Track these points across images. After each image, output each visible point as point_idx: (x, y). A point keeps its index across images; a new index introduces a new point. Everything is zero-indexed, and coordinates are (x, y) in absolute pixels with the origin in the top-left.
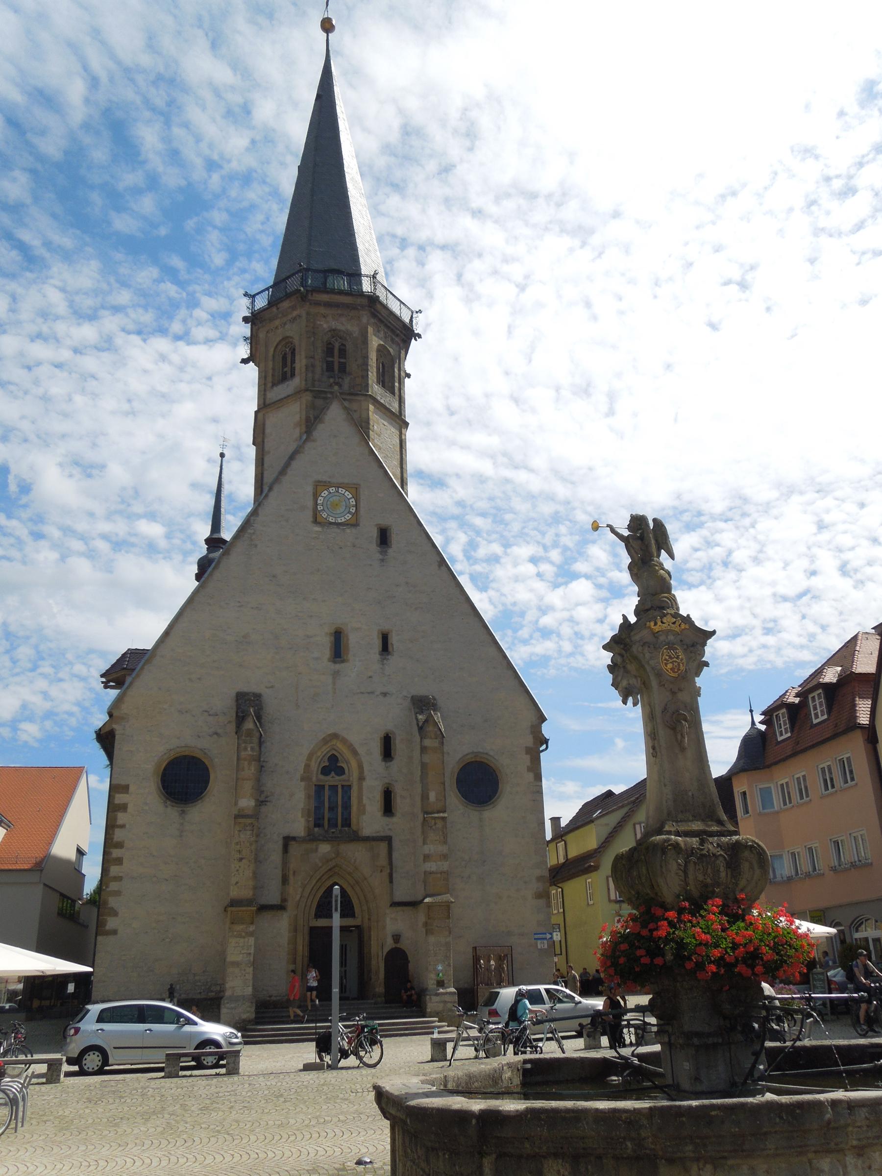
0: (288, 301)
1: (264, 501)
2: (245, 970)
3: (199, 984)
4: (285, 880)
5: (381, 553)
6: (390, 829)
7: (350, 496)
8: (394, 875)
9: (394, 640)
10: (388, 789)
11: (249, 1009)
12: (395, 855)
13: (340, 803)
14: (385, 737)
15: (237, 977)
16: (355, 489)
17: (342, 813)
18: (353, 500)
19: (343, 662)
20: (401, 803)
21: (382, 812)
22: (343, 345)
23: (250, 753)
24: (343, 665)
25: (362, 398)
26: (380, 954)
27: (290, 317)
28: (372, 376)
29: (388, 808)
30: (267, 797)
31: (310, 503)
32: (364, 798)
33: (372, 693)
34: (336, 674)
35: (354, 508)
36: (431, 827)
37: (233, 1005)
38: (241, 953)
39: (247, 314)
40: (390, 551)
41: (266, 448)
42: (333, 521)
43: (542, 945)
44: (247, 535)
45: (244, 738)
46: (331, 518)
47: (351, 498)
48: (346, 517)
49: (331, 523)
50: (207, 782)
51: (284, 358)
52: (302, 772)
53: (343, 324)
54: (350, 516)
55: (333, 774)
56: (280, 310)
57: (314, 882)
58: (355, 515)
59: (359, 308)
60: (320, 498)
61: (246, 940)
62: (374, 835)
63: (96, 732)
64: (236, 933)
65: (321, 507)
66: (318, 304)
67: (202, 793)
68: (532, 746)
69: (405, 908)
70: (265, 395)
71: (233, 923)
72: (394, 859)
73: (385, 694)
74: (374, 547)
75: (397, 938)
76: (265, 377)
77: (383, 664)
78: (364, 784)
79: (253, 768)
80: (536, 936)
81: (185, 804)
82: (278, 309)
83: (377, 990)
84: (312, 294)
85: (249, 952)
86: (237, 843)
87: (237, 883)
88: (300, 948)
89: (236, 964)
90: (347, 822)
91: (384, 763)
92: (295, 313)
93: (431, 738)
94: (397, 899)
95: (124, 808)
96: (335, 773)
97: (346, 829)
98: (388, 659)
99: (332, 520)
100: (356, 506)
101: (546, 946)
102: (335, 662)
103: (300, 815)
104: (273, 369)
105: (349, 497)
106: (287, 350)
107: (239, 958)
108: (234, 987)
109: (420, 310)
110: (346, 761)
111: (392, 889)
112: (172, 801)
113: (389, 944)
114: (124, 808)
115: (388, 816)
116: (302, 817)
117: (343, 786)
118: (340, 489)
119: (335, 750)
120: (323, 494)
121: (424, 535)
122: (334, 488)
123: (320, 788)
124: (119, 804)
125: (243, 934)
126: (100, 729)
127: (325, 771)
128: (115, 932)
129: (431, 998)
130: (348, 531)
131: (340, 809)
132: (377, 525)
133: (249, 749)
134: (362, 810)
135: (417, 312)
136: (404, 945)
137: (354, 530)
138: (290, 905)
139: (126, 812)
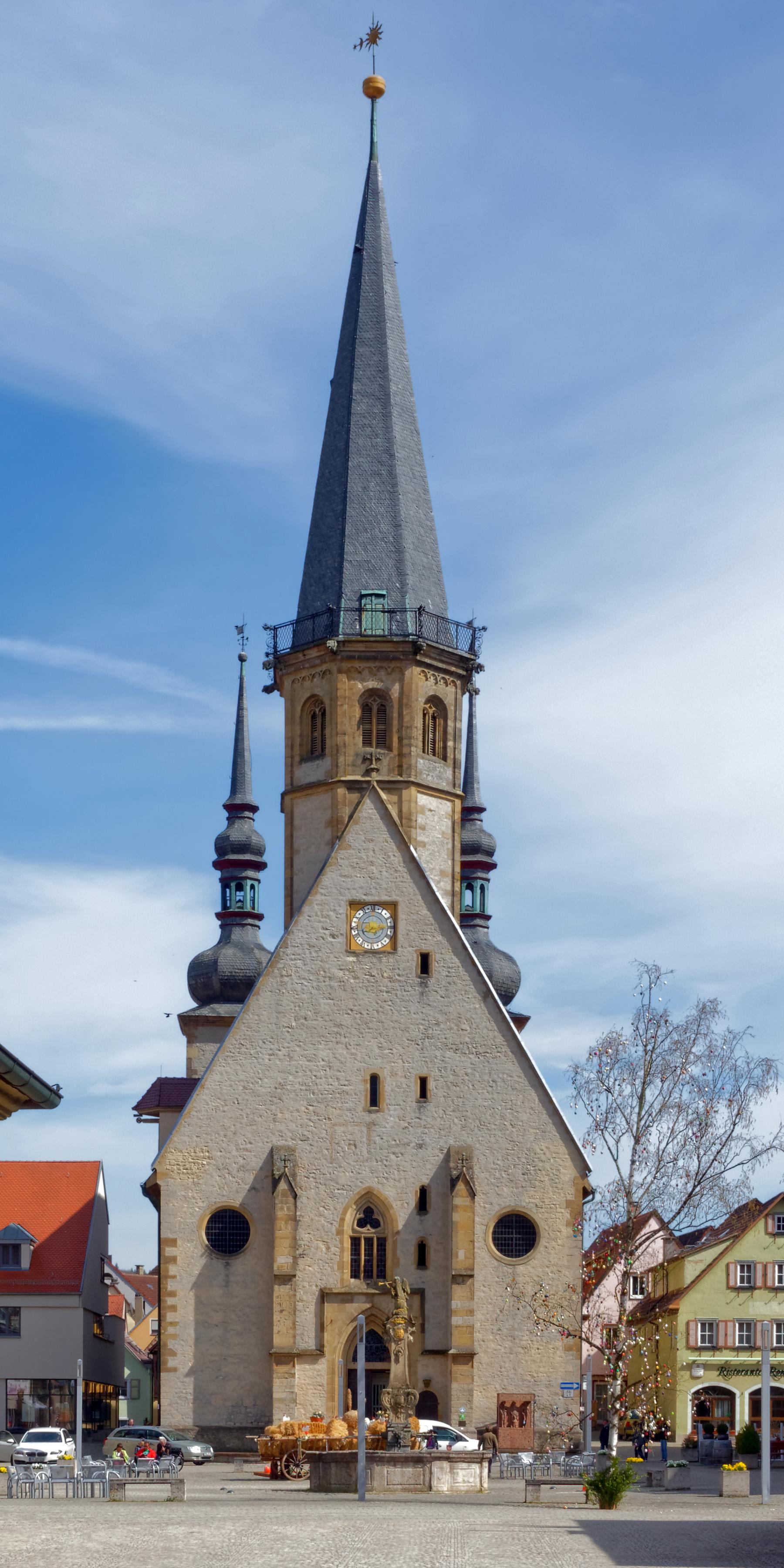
0: (316, 649)
3: (250, 1415)
4: (321, 1328)
6: (423, 1282)
8: (426, 1325)
9: (431, 1085)
10: (422, 1242)
12: (428, 1307)
16: (392, 906)
19: (377, 1111)
20: (432, 1256)
22: (382, 705)
24: (378, 1115)
25: (404, 785)
27: (318, 670)
28: (416, 749)
29: (422, 1261)
31: (343, 928)
32: (398, 1252)
34: (371, 1125)
40: (432, 982)
47: (388, 918)
48: (383, 941)
49: (367, 952)
50: (248, 1235)
51: (314, 717)
52: (337, 1226)
55: (368, 1227)
56: (307, 657)
59: (402, 657)
61: (289, 1380)
63: (141, 1186)
66: (350, 658)
67: (244, 1245)
69: (437, 1357)
70: (292, 771)
72: (426, 1312)
73: (420, 1146)
75: (427, 1382)
76: (292, 747)
77: (420, 1113)
79: (289, 1227)
80: (563, 1386)
81: (229, 1256)
82: (304, 655)
84: (344, 645)
88: (336, 1387)
89: (281, 1400)
90: (382, 1275)
91: (418, 1217)
92: (324, 667)
93: (463, 1197)
94: (430, 1346)
95: (173, 1260)
96: (371, 1226)
98: (425, 1107)
99: (367, 946)
101: (572, 1395)
102: (370, 1112)
103: (336, 1267)
104: (301, 736)
105: (386, 917)
106: (317, 710)
107: (283, 1395)
110: (381, 1213)
111: (424, 1338)
112: (217, 1254)
114: (173, 1260)
116: (338, 1269)
117: (378, 1239)
119: (371, 1203)
120: (357, 915)
121: (469, 961)
122: (369, 907)
123: (355, 1241)
126: (145, 1184)
127: (361, 1223)
128: (175, 1370)
130: (384, 959)
132: (416, 951)
134: (396, 1264)
136: (434, 1388)
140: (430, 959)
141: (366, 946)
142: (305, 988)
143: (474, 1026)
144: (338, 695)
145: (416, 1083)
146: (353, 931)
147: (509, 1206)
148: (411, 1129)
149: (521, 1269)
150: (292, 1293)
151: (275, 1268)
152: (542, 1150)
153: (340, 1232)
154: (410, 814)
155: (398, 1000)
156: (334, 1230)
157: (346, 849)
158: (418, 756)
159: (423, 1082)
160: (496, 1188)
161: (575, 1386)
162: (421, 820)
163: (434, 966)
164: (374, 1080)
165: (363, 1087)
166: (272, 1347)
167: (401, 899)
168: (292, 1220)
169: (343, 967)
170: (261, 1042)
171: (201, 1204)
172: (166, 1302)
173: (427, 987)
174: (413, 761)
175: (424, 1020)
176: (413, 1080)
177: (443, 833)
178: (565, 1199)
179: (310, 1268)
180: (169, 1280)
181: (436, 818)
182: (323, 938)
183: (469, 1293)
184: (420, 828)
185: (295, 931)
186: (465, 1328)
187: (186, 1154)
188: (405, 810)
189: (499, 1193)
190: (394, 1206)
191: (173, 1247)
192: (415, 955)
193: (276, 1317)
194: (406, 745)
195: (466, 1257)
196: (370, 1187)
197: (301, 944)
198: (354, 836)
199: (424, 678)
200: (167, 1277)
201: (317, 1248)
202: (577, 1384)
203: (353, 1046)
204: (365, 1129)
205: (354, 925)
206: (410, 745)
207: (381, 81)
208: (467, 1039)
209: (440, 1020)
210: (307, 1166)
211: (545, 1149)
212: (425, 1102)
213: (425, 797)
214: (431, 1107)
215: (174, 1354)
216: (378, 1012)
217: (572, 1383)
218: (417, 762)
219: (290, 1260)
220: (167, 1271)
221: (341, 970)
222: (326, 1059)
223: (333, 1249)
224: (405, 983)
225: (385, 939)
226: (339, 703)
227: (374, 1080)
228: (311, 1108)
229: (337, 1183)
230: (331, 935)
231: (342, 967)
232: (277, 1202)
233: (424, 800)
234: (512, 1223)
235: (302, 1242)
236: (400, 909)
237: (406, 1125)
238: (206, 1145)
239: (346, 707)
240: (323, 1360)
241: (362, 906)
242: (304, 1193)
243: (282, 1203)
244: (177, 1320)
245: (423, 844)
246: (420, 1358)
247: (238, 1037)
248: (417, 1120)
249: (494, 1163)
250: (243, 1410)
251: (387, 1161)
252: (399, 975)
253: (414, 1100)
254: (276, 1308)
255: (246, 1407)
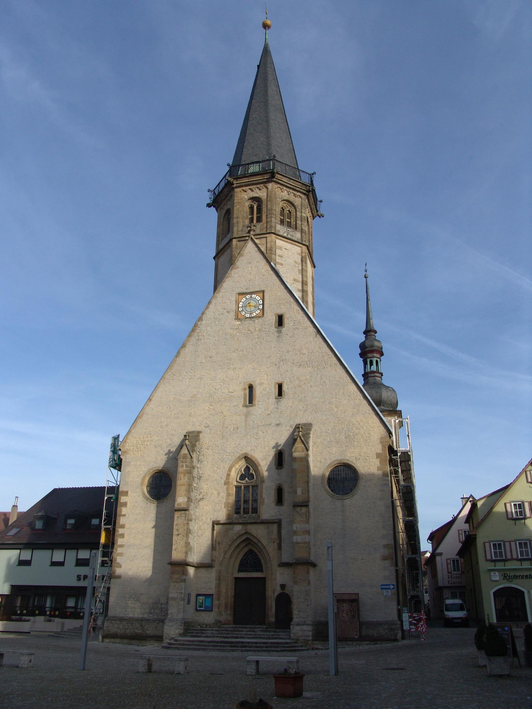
1: (206, 311)
2: (179, 603)
5: (278, 332)
7: (259, 298)
8: (283, 545)
9: (285, 388)
10: (280, 487)
11: (180, 627)
12: (283, 532)
13: (251, 498)
14: (278, 453)
15: (174, 607)
17: (252, 504)
18: (261, 301)
20: (286, 496)
21: (275, 503)
23: (185, 468)
24: (252, 408)
26: (273, 597)
29: (279, 500)
30: (203, 496)
31: (234, 307)
33: (270, 425)
34: (247, 415)
35: (262, 306)
36: (298, 512)
37: (171, 624)
38: (177, 593)
39: (209, 201)
40: (284, 330)
41: (218, 279)
42: (249, 316)
43: (387, 593)
44: (196, 334)
45: (182, 460)
46: (247, 314)
47: (260, 300)
49: (246, 318)
52: (225, 479)
53: (257, 193)
54: (259, 311)
57: (233, 549)
58: (262, 311)
60: (241, 303)
62: (270, 518)
64: (174, 580)
65: (242, 308)
68: (381, 452)
71: (172, 573)
73: (278, 425)
74: (273, 329)
75: (283, 586)
77: (278, 405)
78: (264, 484)
79: (186, 478)
80: (383, 587)
83: (270, 619)
85: (181, 592)
86: (177, 524)
87: (176, 549)
89: (174, 599)
90: (255, 510)
97: (254, 515)
98: (281, 401)
99: (248, 315)
100: (263, 304)
101: (390, 594)
102: (247, 406)
103: (223, 506)
105: (258, 299)
108: (172, 613)
109: (314, 172)
113: (278, 590)
115: (279, 505)
116: (225, 508)
117: (253, 486)
118: (253, 295)
120: (242, 301)
122: (249, 295)
124: (123, 502)
125: (178, 581)
127: (242, 477)
129: (293, 627)
130: (257, 321)
131: (250, 502)
132: (275, 314)
133: (184, 466)
135: (313, 174)
137: (260, 320)
138: (216, 564)
139: (126, 507)
140: (283, 317)
141: (247, 316)
142: (211, 341)
143: (310, 351)
144: (235, 202)
145: (275, 388)
146: (240, 309)
147: (337, 460)
148: (272, 414)
149: (347, 502)
150: (185, 522)
151: (176, 506)
152: (358, 422)
153: (227, 483)
154: (271, 247)
155: (264, 342)
156: (223, 482)
157: (236, 269)
158: (276, 223)
159: (280, 386)
160: (328, 449)
161: (392, 587)
162: (278, 252)
163: (286, 321)
164: (251, 387)
165: (243, 393)
166: (171, 559)
167: (266, 289)
168: (188, 473)
169: (233, 328)
170: (185, 373)
171: (144, 469)
172: (118, 531)
173: (281, 333)
174: (273, 224)
175: (280, 351)
176: (273, 386)
177: (295, 262)
178: (375, 452)
179: (207, 508)
180: (121, 518)
181: (290, 253)
182: (222, 314)
183: (305, 519)
184: (279, 256)
185: (207, 312)
186: (303, 544)
187: (138, 439)
188: (269, 246)
189: (330, 451)
190: (261, 464)
191: (125, 496)
192: (274, 317)
193: (175, 538)
194: (269, 217)
195: (302, 493)
196: (246, 453)
197: (210, 319)
198: (241, 262)
199: (281, 191)
200: (121, 515)
201: (212, 494)
202: (393, 585)
203: (237, 370)
204: (243, 418)
205: (240, 306)
206: (271, 217)
207: (269, 22)
208: (306, 359)
209: (290, 350)
210: (208, 443)
211: (359, 421)
212: (281, 398)
213: (282, 242)
214: (284, 401)
215: (120, 566)
216: (252, 349)
217: (389, 585)
218: (276, 225)
219: (186, 500)
220: (121, 512)
221: (232, 329)
222: (221, 378)
223: (222, 494)
224: (268, 332)
225: (258, 311)
226: (235, 205)
227: (251, 387)
228: (211, 407)
229: (226, 452)
230: (227, 312)
231: (232, 328)
232: (179, 462)
233: (280, 243)
234: (341, 471)
235: (202, 491)
236: (265, 294)
237: (269, 413)
238: (150, 433)
239: (238, 206)
240: (214, 570)
241: (245, 296)
242: (205, 459)
243: (182, 462)
244: (124, 544)
245: (282, 265)
246: (278, 569)
247: (172, 371)
248: (277, 409)
249: (326, 432)
250: (160, 606)
251: (257, 436)
252: (265, 328)
253: (274, 398)
254: (175, 532)
255: (162, 604)
